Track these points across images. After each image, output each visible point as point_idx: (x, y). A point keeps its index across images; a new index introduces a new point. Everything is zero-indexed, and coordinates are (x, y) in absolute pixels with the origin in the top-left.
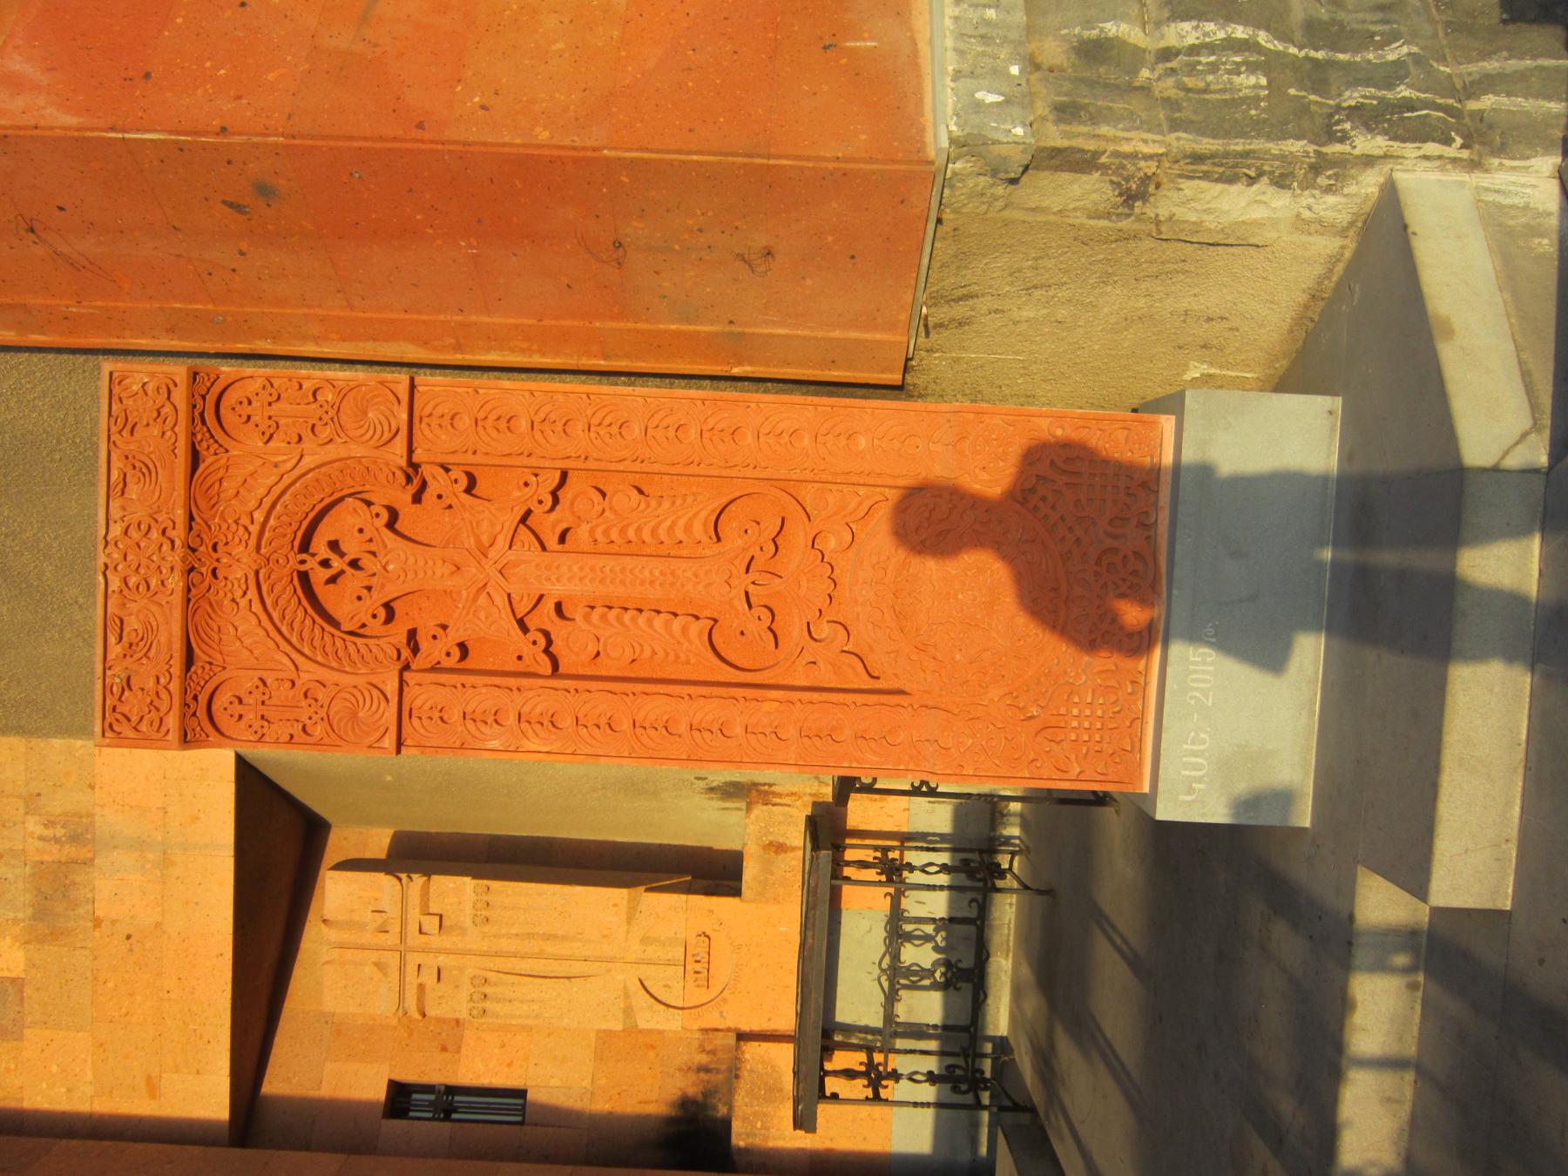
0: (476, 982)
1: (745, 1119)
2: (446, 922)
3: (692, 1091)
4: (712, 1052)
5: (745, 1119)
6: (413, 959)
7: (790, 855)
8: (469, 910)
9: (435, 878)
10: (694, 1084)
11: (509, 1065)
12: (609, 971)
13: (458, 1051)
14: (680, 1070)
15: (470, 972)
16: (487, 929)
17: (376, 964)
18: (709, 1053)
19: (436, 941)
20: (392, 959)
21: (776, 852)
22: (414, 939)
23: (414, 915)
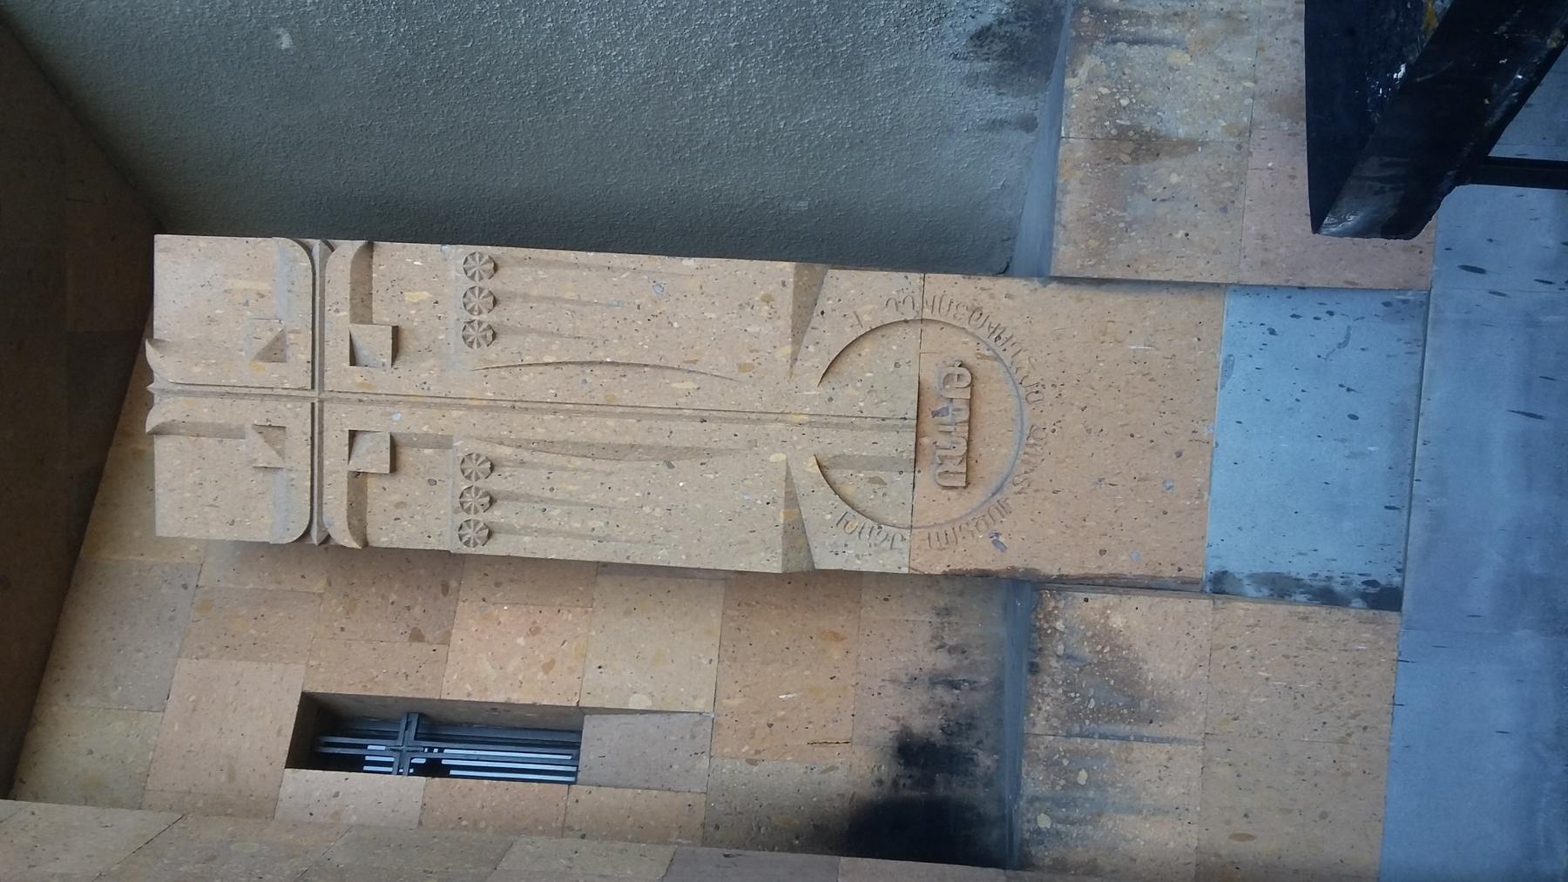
0: (471, 466)
1: (1051, 764)
2: (409, 344)
3: (921, 724)
4: (960, 650)
5: (1051, 764)
6: (338, 422)
7: (1166, 162)
8: (455, 315)
9: (384, 248)
10: (926, 711)
11: (547, 668)
12: (753, 444)
13: (446, 640)
14: (893, 681)
15: (461, 446)
16: (493, 353)
17: (261, 429)
18: (951, 650)
19: (386, 379)
20: (296, 420)
21: (1136, 156)
22: (339, 373)
23: (339, 320)
